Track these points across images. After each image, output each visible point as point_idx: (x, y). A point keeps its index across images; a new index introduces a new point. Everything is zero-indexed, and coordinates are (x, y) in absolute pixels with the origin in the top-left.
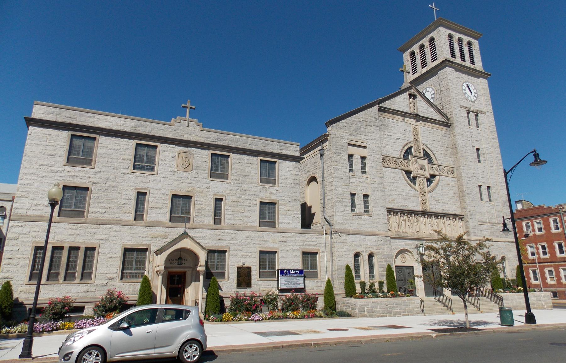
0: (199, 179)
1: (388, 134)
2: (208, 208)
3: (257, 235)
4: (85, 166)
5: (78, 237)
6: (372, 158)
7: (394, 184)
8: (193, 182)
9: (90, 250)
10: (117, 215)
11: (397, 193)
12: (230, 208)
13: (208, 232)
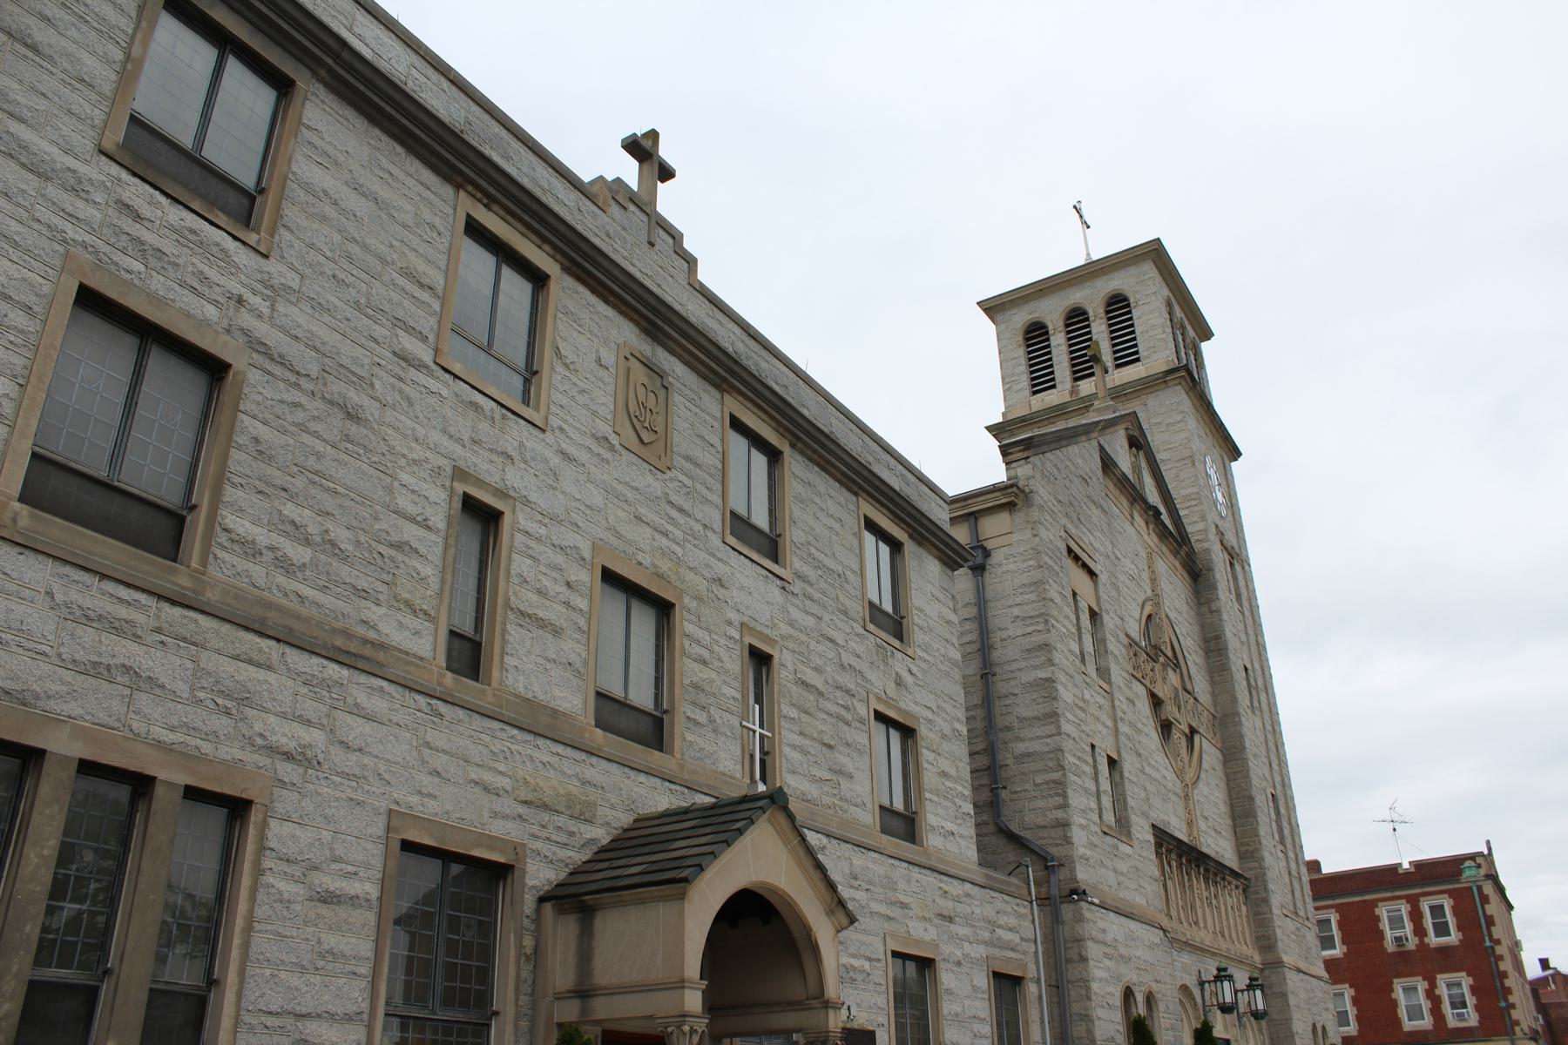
5: (143, 700)
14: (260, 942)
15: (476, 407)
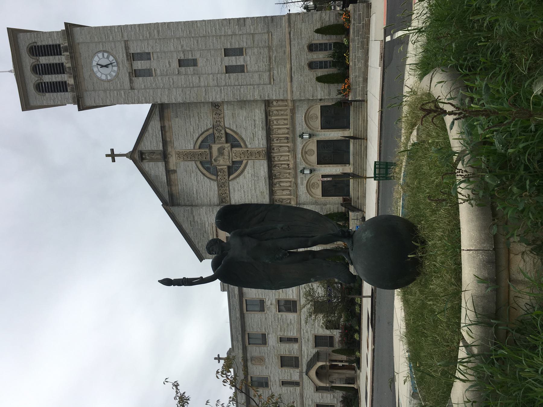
0: (268, 352)
1: (195, 192)
2: (288, 347)
3: (303, 315)
8: (271, 355)
10: (298, 394)
11: (253, 188)
12: (286, 333)
13: (303, 347)
14: (326, 402)
15: (272, 385)
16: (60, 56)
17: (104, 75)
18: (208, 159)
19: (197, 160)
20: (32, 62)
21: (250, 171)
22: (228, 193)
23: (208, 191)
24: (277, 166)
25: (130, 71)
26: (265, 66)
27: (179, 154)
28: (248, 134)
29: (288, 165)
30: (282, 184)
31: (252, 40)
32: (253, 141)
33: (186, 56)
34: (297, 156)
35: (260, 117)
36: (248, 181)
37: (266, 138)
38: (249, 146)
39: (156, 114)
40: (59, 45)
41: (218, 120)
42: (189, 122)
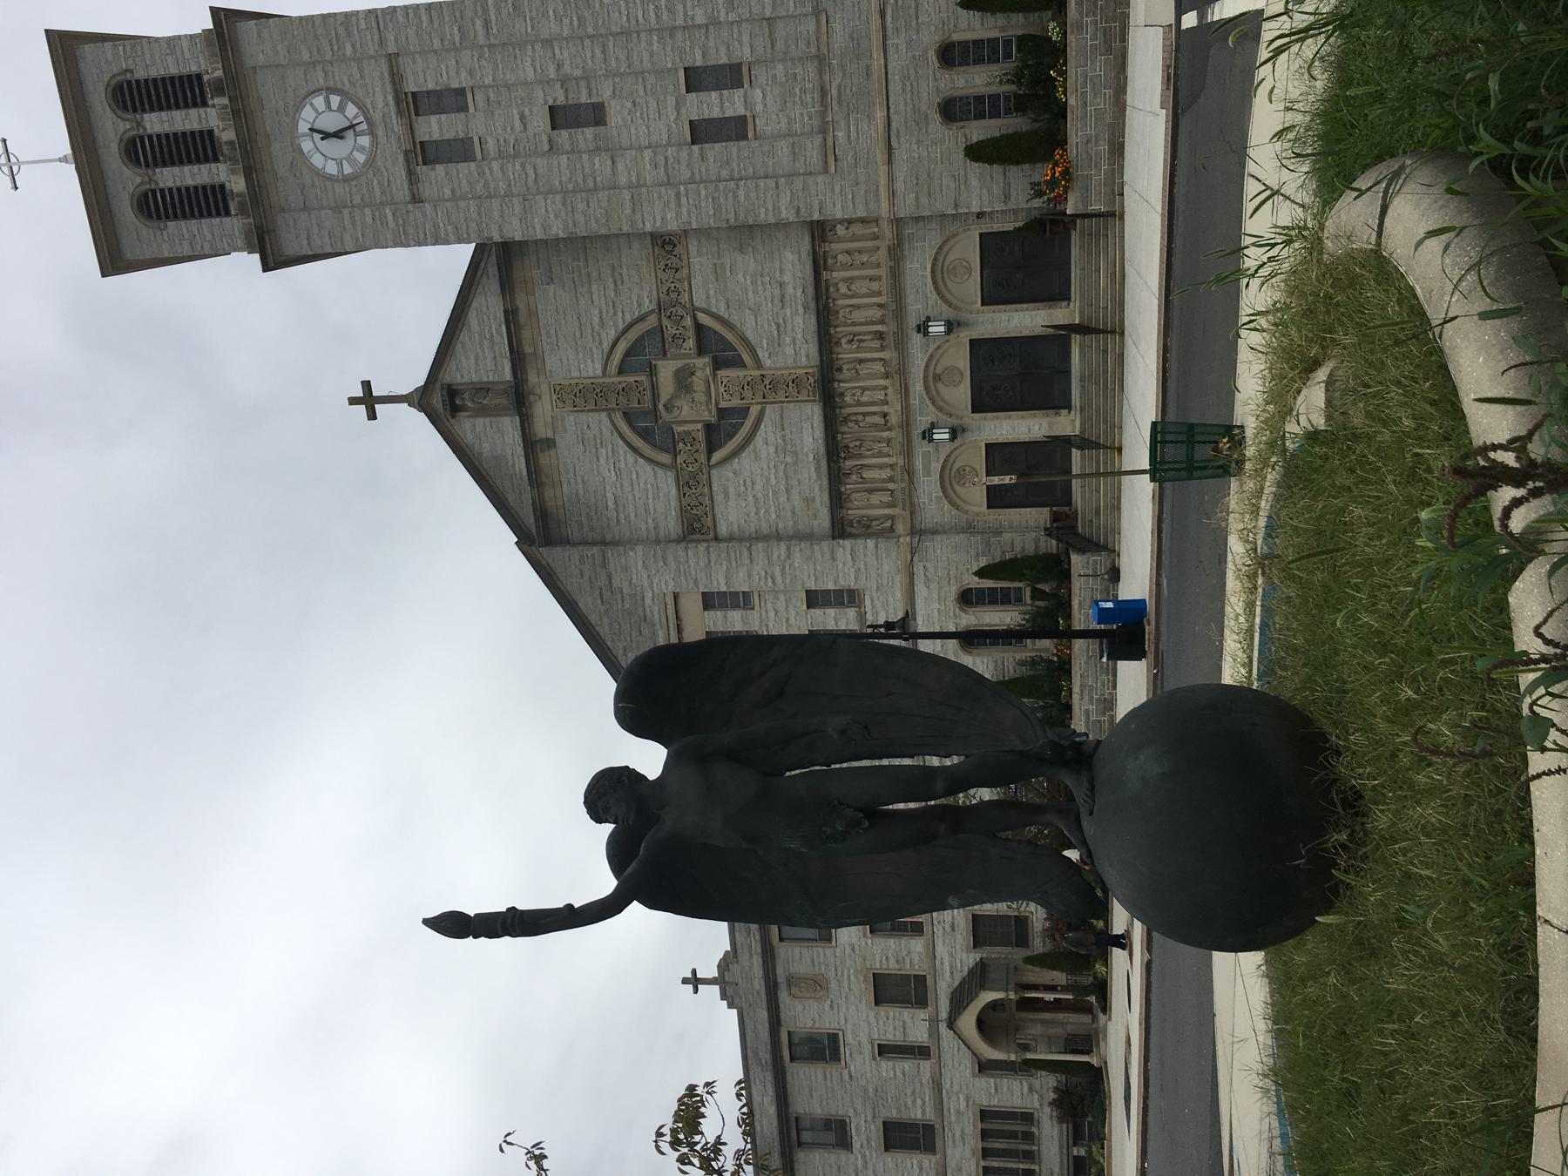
1: (610, 503)
4: (848, 1128)
5: (966, 1132)
6: (702, 577)
7: (760, 495)
8: (846, 972)
9: (985, 1115)
11: (782, 487)
13: (940, 948)
14: (1009, 1104)
15: (851, 1055)
16: (202, 110)
17: (334, 162)
18: (647, 403)
19: (614, 409)
20: (122, 129)
21: (771, 438)
22: (708, 502)
23: (650, 501)
24: (851, 421)
25: (408, 148)
26: (811, 118)
27: (559, 391)
28: (762, 326)
29: (885, 415)
30: (867, 474)
31: (767, 39)
32: (779, 345)
33: (571, 96)
34: (912, 390)
35: (799, 274)
36: (765, 467)
37: (815, 335)
38: (768, 363)
39: (491, 274)
40: (199, 77)
41: (673, 285)
42: (587, 295)
